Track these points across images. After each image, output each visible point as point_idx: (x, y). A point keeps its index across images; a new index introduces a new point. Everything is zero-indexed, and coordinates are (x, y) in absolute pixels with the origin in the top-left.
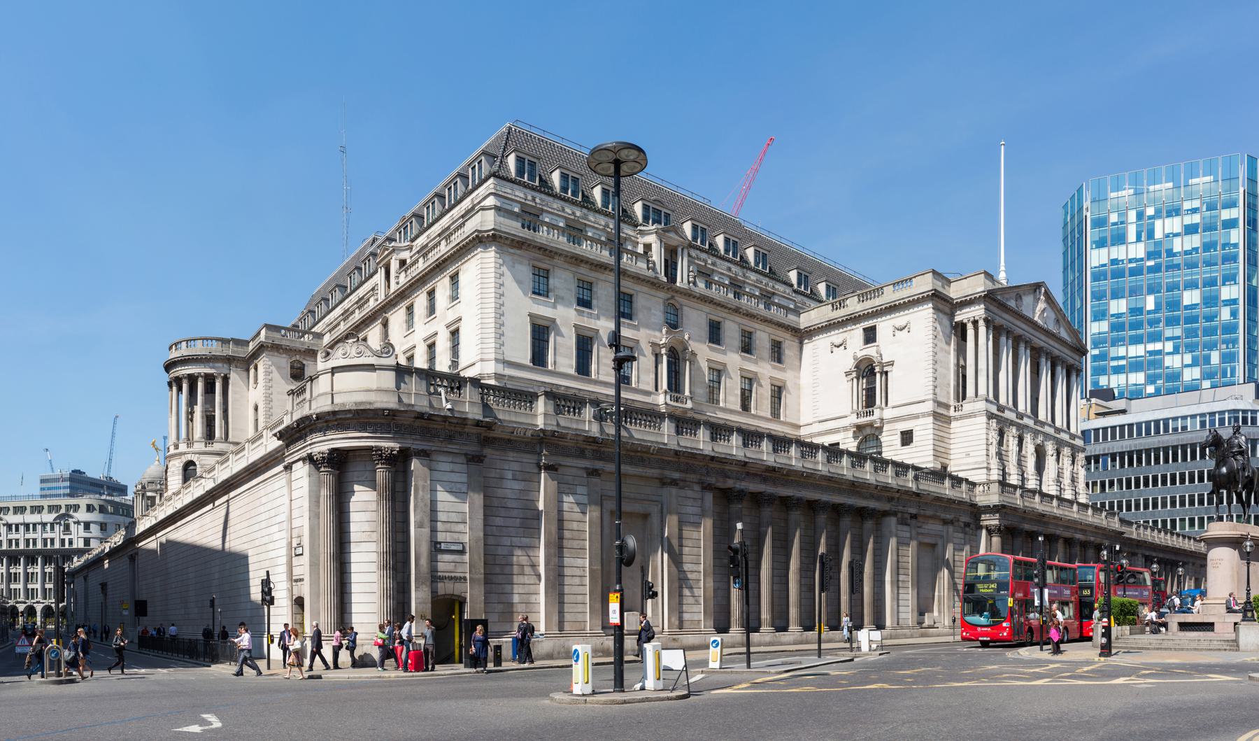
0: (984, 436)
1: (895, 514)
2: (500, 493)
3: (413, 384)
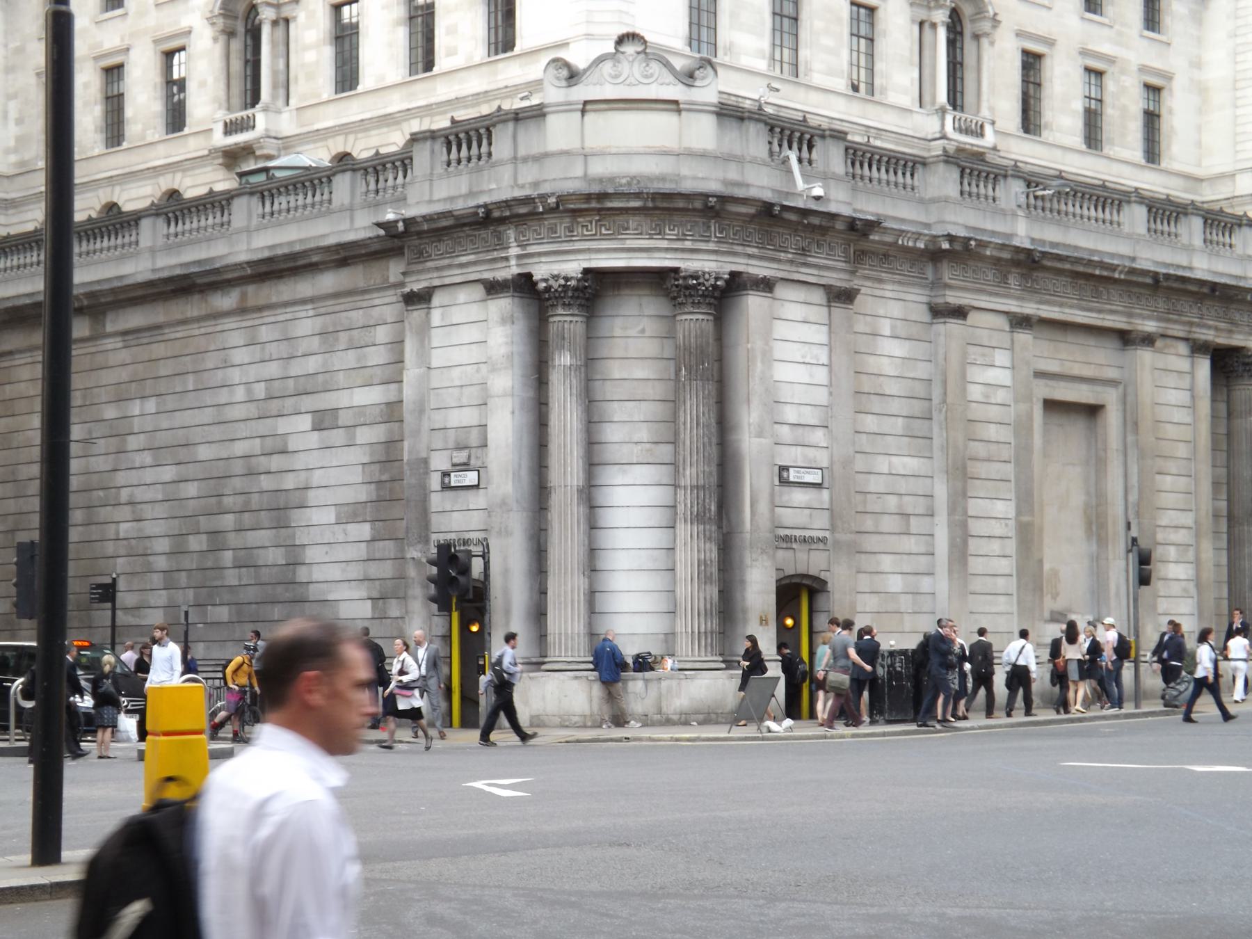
3: (755, 142)
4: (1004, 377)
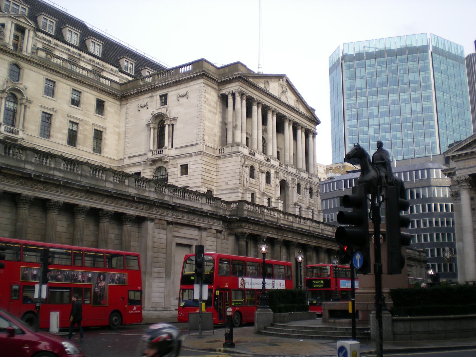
0: (238, 170)
1: (152, 220)
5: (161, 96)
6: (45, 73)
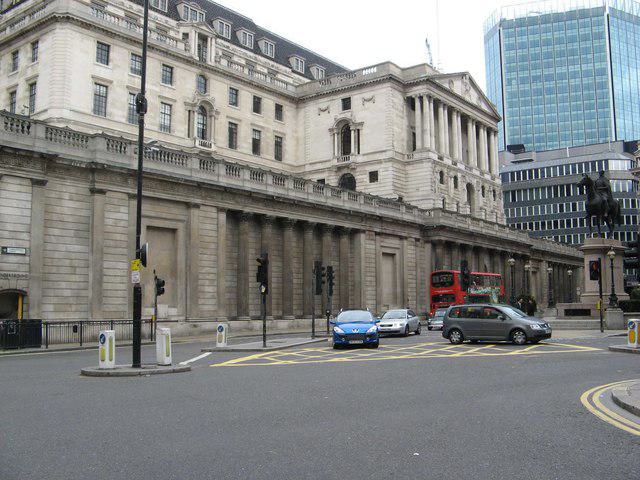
0: (429, 177)
1: (364, 232)
2: (58, 209)
4: (125, 217)
5: (343, 100)
6: (229, 82)
